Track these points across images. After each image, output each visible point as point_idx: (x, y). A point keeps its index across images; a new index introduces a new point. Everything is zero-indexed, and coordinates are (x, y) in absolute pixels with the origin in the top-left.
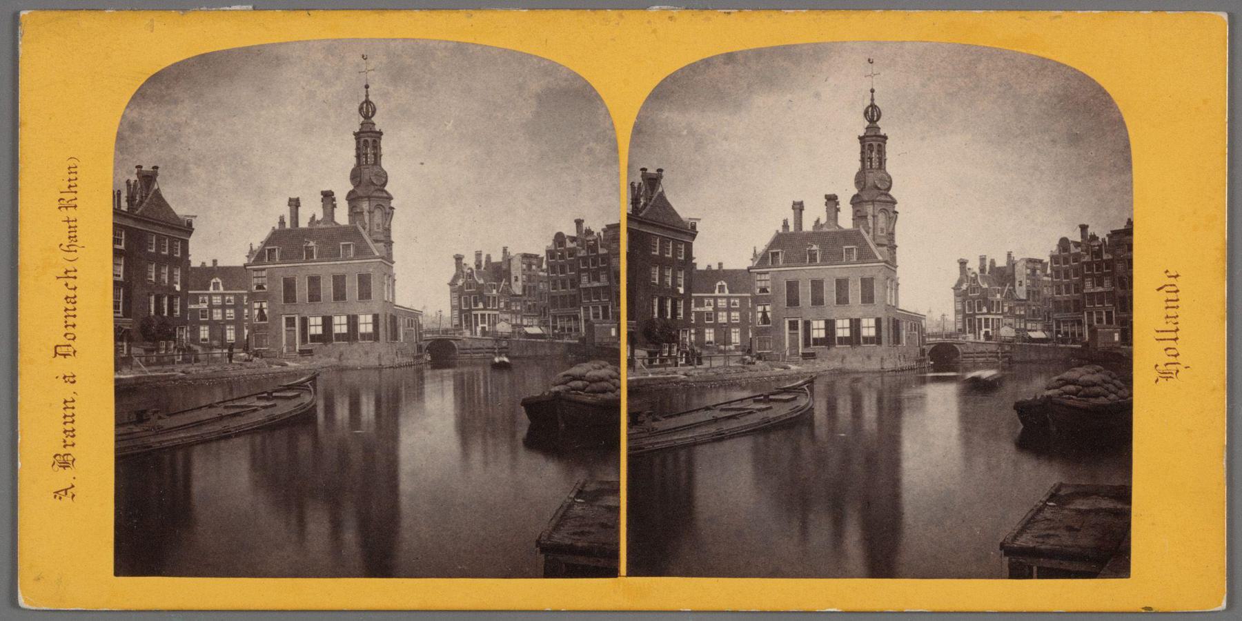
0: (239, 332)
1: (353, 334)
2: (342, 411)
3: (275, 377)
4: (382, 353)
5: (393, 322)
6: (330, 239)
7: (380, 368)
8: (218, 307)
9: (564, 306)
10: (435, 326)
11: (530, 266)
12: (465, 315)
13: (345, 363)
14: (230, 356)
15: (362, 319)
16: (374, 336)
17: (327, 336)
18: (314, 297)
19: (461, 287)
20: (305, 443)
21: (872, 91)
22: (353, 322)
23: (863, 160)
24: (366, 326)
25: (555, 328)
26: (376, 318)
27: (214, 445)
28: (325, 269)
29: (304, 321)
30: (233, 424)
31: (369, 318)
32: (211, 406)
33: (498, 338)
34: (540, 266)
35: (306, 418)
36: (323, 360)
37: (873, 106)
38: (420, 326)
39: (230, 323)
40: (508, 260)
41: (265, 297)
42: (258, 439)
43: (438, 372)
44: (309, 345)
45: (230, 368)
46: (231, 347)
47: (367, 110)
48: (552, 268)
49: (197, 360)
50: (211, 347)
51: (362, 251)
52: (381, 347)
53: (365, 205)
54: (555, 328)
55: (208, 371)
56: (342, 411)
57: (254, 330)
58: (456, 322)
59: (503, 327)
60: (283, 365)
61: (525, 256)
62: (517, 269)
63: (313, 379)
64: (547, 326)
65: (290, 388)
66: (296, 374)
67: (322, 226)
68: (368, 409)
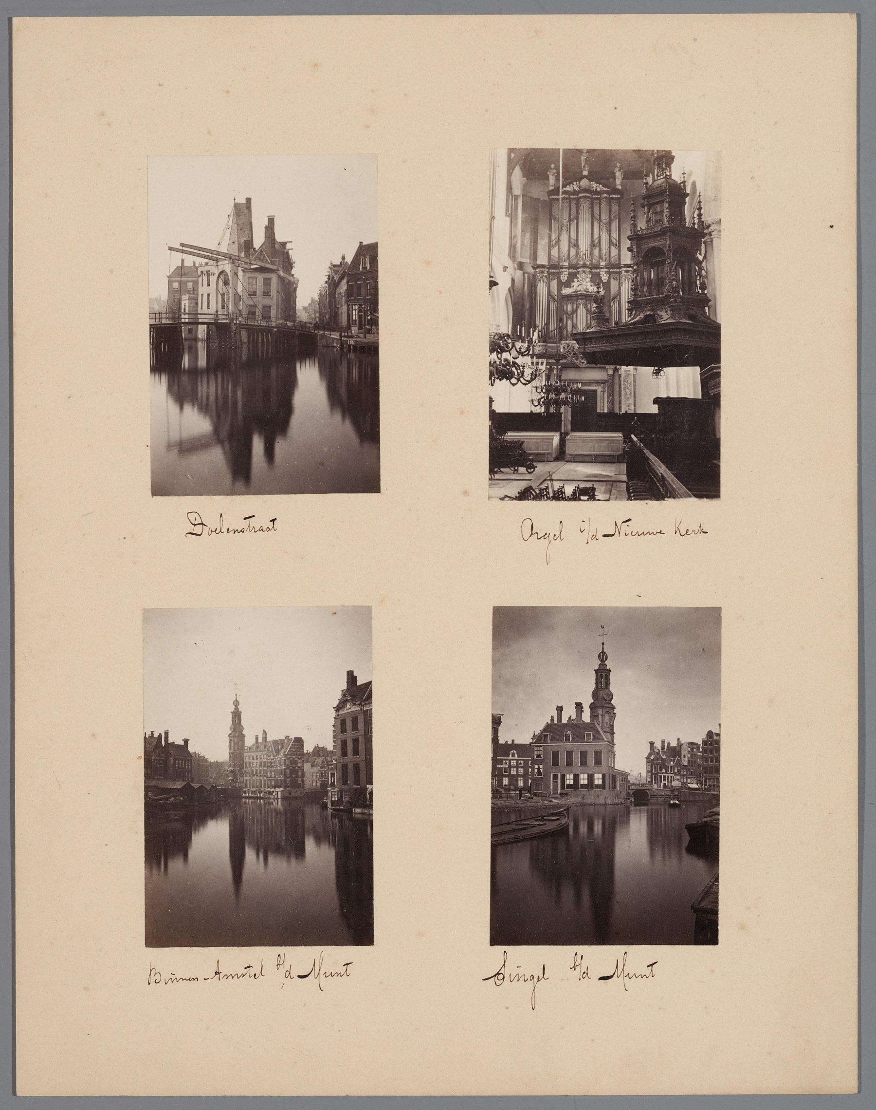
0: (525, 782)
1: (590, 785)
2: (583, 828)
3: (546, 807)
4: (605, 797)
5: (613, 778)
6: (577, 730)
7: (605, 805)
8: (514, 767)
9: (711, 773)
10: (637, 782)
11: (692, 749)
12: (654, 776)
13: (585, 801)
14: (520, 796)
15: (596, 776)
16: (603, 786)
17: (576, 785)
18: (584, 762)
19: (653, 760)
20: (562, 846)
21: (603, 644)
22: (591, 778)
23: (597, 683)
24: (598, 781)
25: (706, 785)
26: (604, 776)
27: (509, 846)
28: (576, 747)
29: (563, 776)
30: (520, 834)
31: (600, 776)
32: (508, 824)
33: (673, 789)
34: (698, 749)
35: (562, 832)
36: (572, 800)
37: (603, 652)
38: (629, 781)
39: (521, 776)
40: (680, 745)
41: (541, 762)
42: (535, 843)
43: (638, 808)
44: (566, 790)
45: (520, 802)
46: (521, 790)
47: (603, 657)
48: (705, 751)
49: (501, 797)
50: (509, 790)
51: (597, 737)
52: (606, 792)
53: (600, 711)
54: (706, 785)
55: (507, 803)
56: (583, 828)
57: (534, 780)
58: (649, 780)
59: (676, 784)
60: (551, 801)
61: (690, 743)
62: (685, 751)
63: (568, 809)
64: (701, 784)
65: (553, 814)
66: (557, 806)
67: (575, 722)
68: (598, 828)
